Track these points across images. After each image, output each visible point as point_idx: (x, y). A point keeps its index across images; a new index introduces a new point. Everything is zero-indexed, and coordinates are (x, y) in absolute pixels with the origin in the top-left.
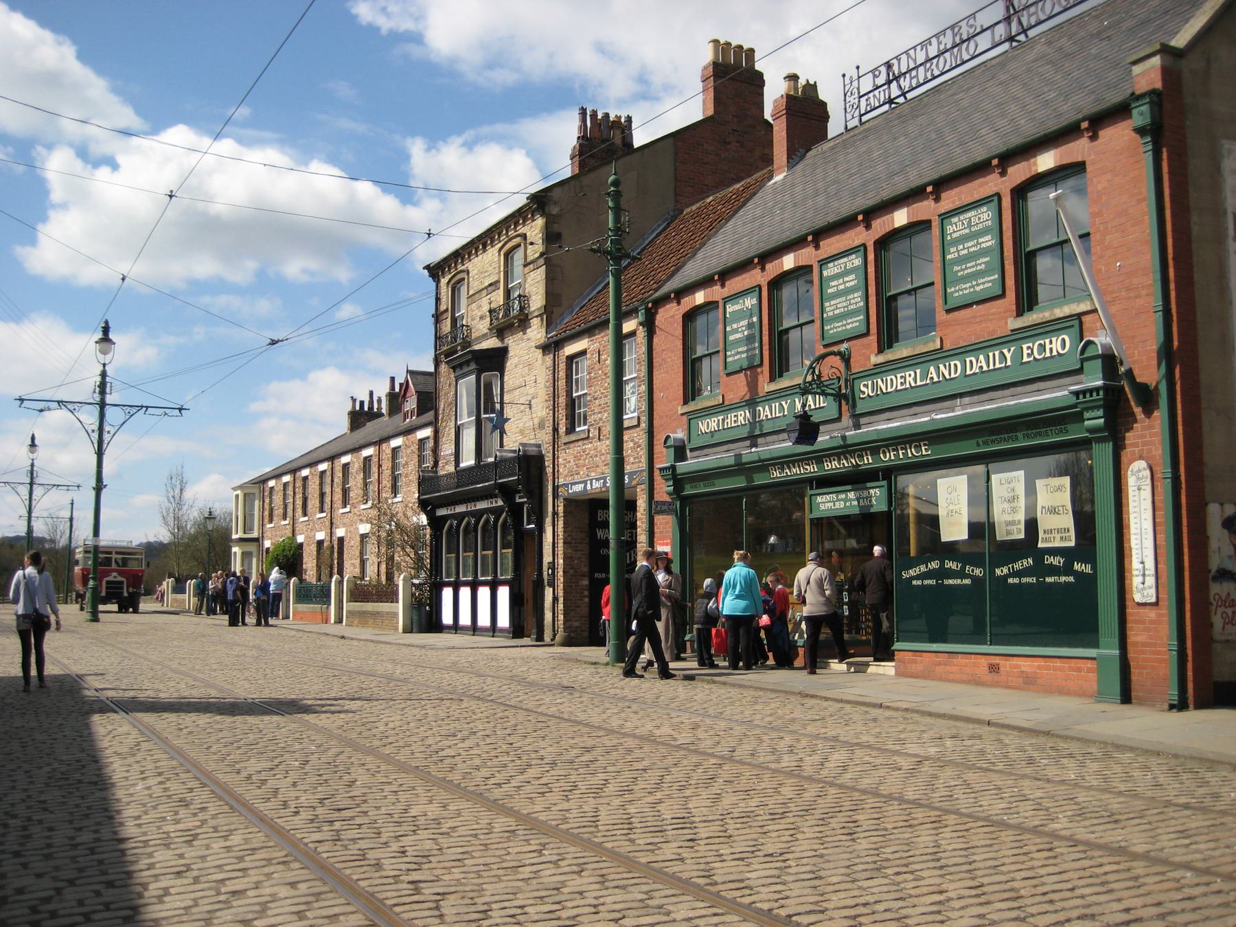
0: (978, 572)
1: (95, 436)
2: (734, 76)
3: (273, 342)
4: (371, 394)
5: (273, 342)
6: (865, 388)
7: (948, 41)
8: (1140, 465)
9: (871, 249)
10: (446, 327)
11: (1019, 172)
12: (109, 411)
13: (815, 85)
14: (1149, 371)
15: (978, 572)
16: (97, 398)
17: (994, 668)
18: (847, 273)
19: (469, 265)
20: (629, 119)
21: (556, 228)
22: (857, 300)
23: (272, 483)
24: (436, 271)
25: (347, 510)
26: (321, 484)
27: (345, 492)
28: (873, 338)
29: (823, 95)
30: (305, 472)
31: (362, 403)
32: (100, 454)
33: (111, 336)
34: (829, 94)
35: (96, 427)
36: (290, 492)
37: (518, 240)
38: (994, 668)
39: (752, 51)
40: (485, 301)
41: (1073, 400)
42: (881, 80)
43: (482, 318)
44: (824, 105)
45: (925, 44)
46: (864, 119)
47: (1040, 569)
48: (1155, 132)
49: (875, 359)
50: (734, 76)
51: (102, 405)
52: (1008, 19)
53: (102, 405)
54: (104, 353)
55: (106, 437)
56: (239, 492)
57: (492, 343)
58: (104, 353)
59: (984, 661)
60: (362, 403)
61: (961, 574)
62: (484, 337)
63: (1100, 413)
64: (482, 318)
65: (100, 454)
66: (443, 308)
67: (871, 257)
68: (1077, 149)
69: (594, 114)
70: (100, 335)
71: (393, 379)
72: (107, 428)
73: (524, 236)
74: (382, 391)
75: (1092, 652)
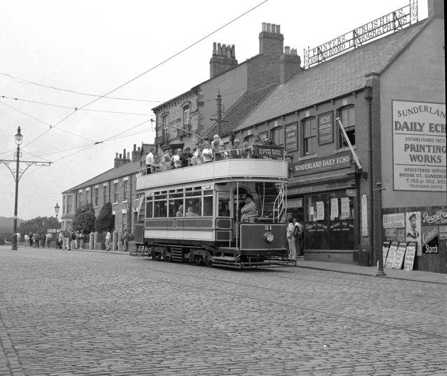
0: (326, 227)
1: (15, 174)
2: (271, 37)
3: (97, 143)
4: (125, 150)
5: (97, 143)
6: (297, 168)
7: (336, 43)
8: (365, 196)
9: (299, 123)
10: (160, 134)
11: (339, 104)
12: (20, 164)
13: (296, 50)
14: (366, 170)
15: (326, 227)
16: (16, 158)
17: (329, 257)
18: (291, 132)
19: (170, 110)
20: (233, 46)
21: (201, 100)
22: (294, 139)
23: (81, 191)
24: (156, 110)
25: (117, 203)
26: (105, 192)
27: (116, 195)
28: (299, 151)
29: (299, 54)
30: (97, 187)
31: (121, 155)
32: (17, 181)
33: (21, 133)
34: (300, 53)
35: (15, 170)
36: (89, 195)
37: (186, 104)
38: (329, 257)
39: (279, 26)
40: (175, 126)
41: (347, 176)
42: (316, 53)
43: (174, 131)
44: (299, 57)
45: (330, 43)
46: (311, 66)
47: (342, 227)
48: (369, 99)
49: (300, 159)
50: (271, 37)
51: (18, 161)
52: (354, 39)
53: (18, 161)
54: (19, 140)
55: (20, 174)
56: (65, 195)
57: (177, 142)
58: (19, 140)
59: (327, 254)
60: (121, 155)
61: (321, 228)
62: (176, 139)
63: (354, 180)
64: (174, 131)
65: (17, 181)
66: (159, 126)
67: (299, 126)
68: (352, 100)
69: (219, 44)
70: (17, 133)
71: (135, 146)
72: (20, 171)
73: (190, 102)
74: (130, 150)
75: (352, 251)
